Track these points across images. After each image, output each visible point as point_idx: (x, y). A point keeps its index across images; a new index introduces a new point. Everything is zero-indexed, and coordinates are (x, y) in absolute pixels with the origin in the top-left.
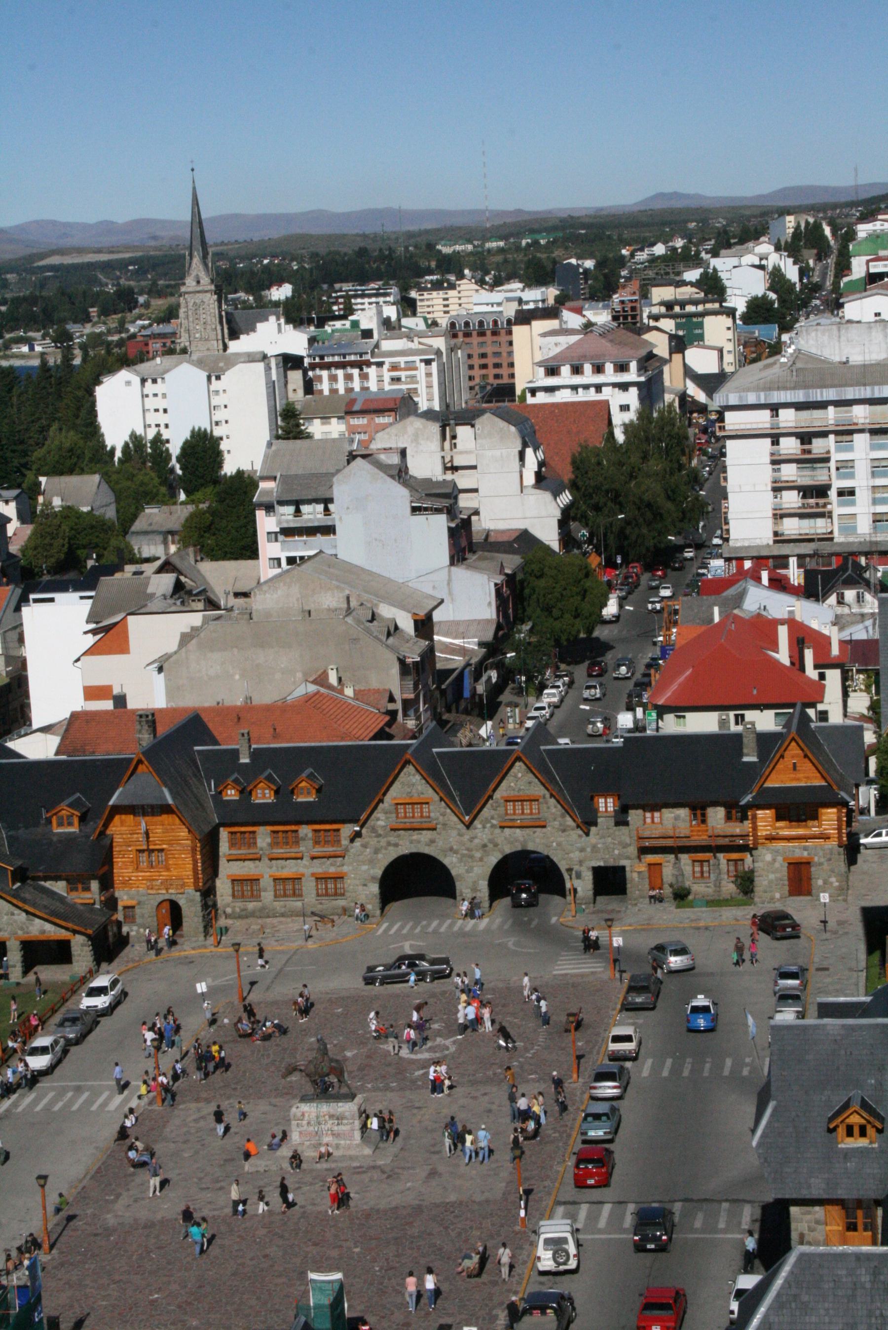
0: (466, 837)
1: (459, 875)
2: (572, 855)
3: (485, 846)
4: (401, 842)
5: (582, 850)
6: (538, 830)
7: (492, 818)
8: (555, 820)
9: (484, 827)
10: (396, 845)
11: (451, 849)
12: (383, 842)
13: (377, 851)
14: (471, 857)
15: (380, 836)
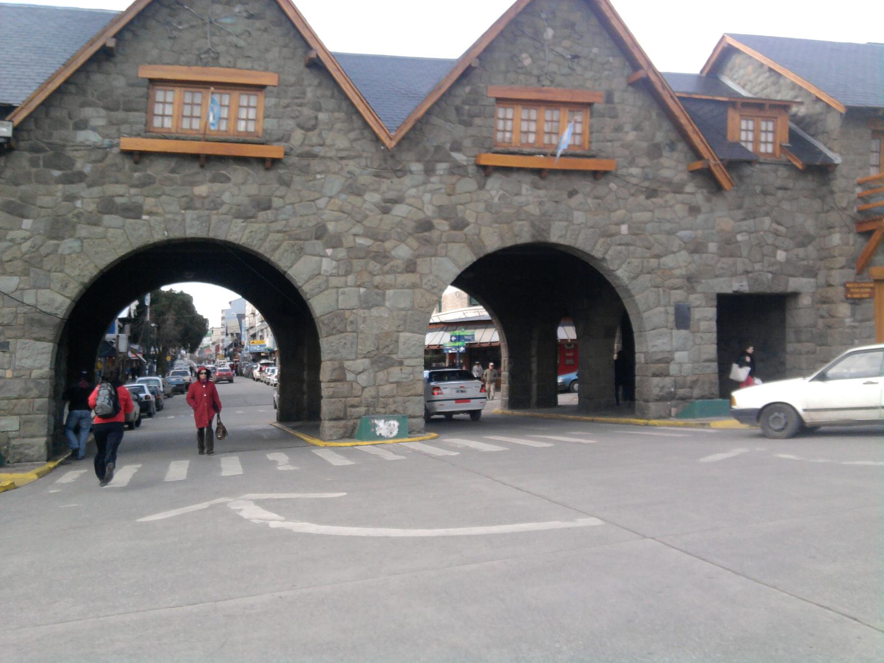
0: (373, 197)
1: (338, 314)
2: (668, 261)
3: (426, 226)
4: (149, 203)
5: (697, 248)
6: (585, 186)
7: (457, 147)
8: (632, 163)
9: (429, 171)
10: (133, 211)
11: (320, 233)
12: (87, 200)
13: (59, 228)
14: (382, 257)
15: (80, 177)
